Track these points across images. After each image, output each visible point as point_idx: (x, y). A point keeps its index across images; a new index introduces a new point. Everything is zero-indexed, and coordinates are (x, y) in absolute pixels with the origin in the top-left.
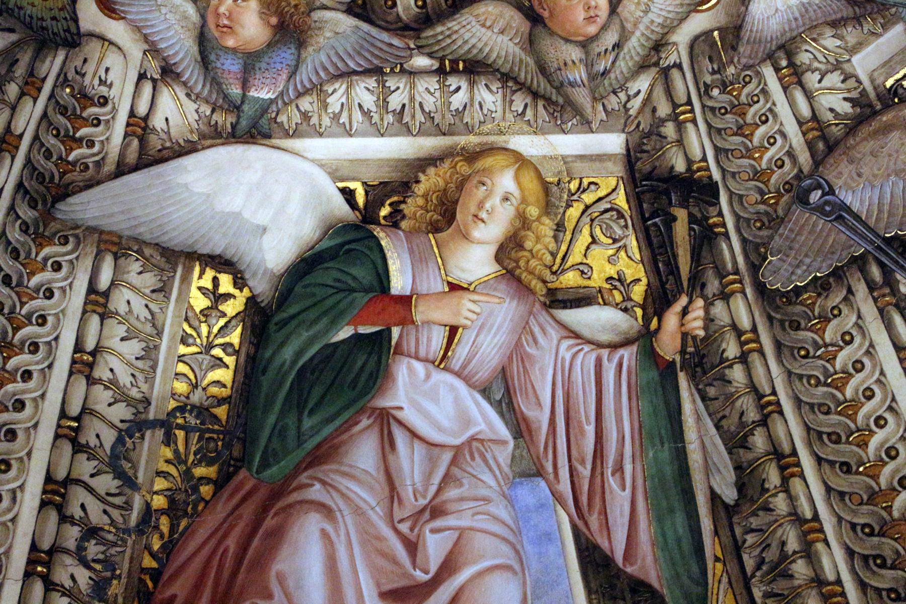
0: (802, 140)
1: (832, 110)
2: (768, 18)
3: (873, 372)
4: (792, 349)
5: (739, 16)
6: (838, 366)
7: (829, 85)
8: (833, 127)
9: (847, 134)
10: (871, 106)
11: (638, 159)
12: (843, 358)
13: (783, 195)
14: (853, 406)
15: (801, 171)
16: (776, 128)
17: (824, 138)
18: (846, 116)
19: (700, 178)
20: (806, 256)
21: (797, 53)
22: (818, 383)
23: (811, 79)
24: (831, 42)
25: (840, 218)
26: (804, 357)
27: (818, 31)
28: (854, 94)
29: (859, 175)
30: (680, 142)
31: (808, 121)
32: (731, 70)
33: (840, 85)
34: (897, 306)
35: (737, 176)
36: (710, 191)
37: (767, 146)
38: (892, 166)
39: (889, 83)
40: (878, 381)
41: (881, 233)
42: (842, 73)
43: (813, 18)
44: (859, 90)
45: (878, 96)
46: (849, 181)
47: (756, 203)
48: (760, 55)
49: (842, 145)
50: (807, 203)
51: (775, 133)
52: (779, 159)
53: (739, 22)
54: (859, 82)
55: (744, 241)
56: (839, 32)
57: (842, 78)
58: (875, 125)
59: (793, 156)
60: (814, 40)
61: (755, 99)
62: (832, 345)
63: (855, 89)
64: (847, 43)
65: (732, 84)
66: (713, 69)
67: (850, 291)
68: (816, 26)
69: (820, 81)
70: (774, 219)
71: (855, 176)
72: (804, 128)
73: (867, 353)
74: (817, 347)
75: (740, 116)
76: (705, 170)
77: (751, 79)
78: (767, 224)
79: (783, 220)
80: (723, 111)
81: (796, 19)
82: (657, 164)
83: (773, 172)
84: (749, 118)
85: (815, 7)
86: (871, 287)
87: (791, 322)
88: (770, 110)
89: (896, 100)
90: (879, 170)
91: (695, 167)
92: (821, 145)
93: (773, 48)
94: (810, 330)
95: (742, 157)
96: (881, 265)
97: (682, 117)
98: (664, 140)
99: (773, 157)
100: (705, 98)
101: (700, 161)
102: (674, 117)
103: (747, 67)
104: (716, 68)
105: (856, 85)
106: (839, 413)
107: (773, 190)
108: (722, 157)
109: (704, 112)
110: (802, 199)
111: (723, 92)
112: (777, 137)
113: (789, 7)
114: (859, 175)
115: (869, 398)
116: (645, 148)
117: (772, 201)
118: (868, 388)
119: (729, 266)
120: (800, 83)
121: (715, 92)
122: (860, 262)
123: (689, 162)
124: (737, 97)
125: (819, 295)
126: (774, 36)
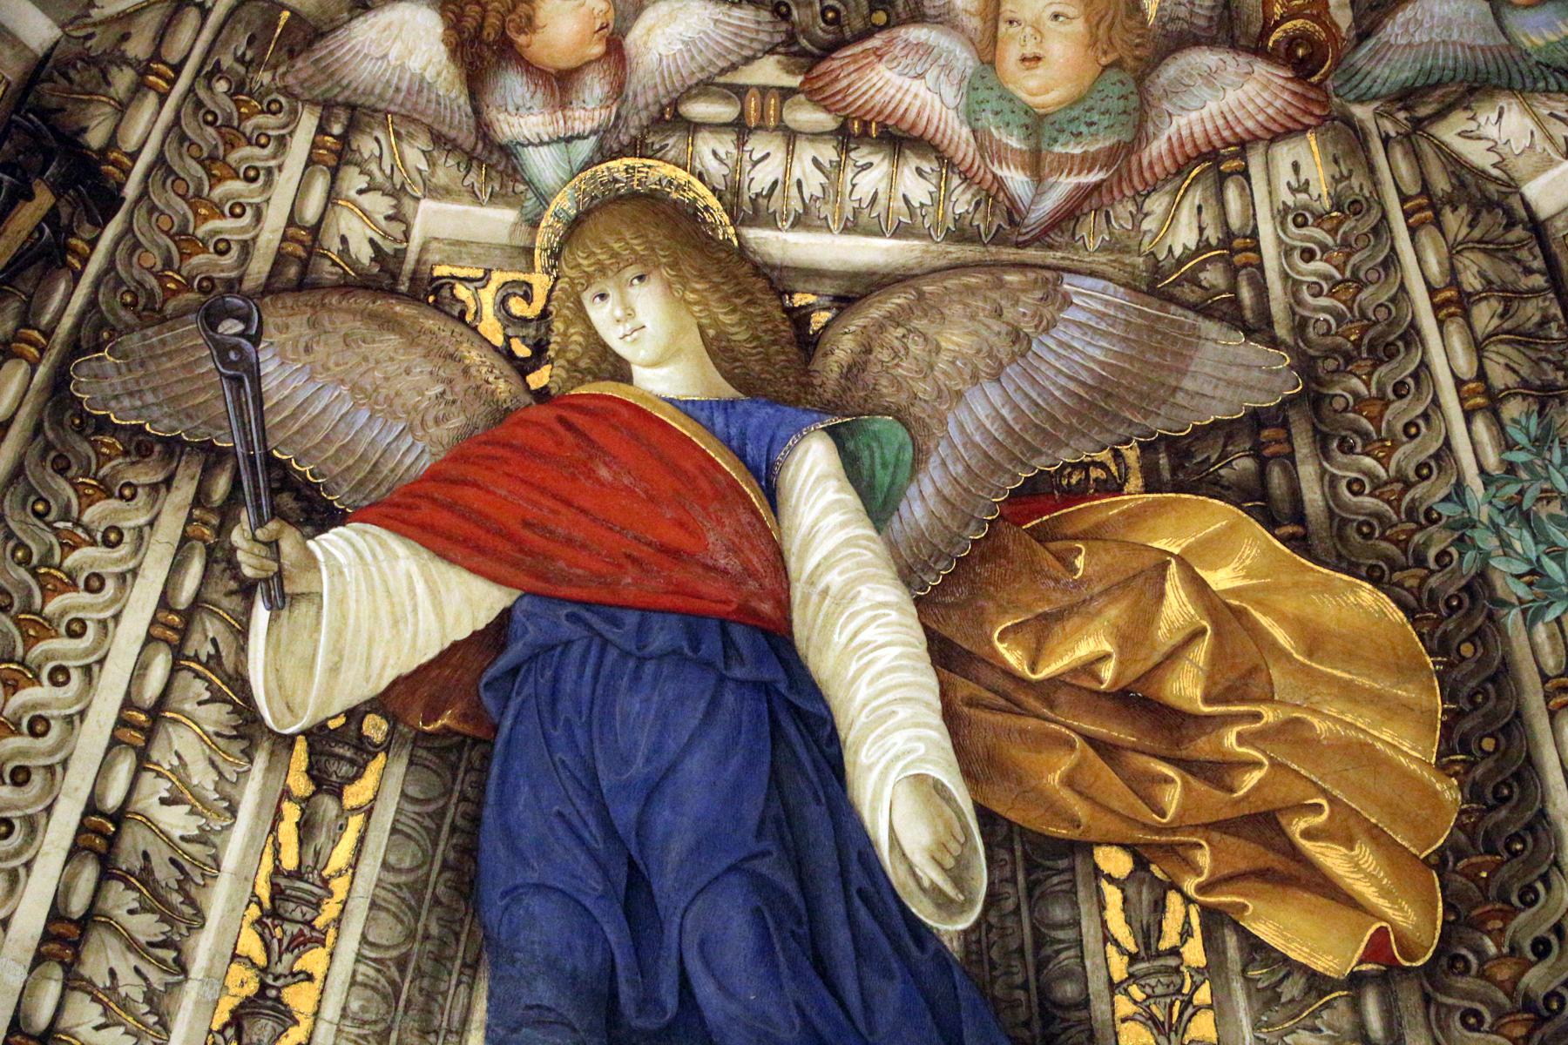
0: (276, 243)
1: (344, 240)
2: (366, 56)
3: (107, 606)
4: (32, 490)
5: (332, 21)
6: (68, 562)
7: (366, 206)
8: (328, 263)
9: (336, 287)
10: (395, 277)
11: (50, 79)
12: (84, 557)
13: (191, 290)
14: (46, 628)
15: (240, 280)
16: (257, 200)
17: (305, 265)
18: (354, 264)
19: (108, 175)
20: (154, 390)
21: (363, 132)
22: (25, 562)
23: (353, 180)
24: (414, 157)
25: (237, 381)
26: (40, 516)
27: (412, 128)
28: (388, 247)
29: (308, 350)
30: (122, 108)
31: (304, 228)
32: (265, 77)
33: (380, 218)
34: (210, 550)
35: (156, 215)
36: (108, 202)
37: (227, 210)
38: (355, 376)
39: (438, 272)
40: (103, 624)
41: (271, 444)
42: (395, 207)
43: (420, 108)
44: (398, 246)
45: (414, 278)
46: (289, 347)
47: (150, 270)
48: (317, 92)
49: (318, 295)
50: (214, 328)
51: (251, 204)
52: (227, 241)
53: (326, 28)
54: (407, 235)
55: (92, 303)
56: (435, 153)
57: (391, 212)
58: (380, 305)
59: (248, 253)
60: (397, 135)
61: (263, 140)
62: (87, 530)
63: (395, 240)
64: (433, 174)
65: (250, 94)
66: (244, 54)
67: (168, 482)
68: (414, 121)
69: (361, 192)
70: (153, 310)
71: (301, 346)
72: (291, 231)
73: (122, 577)
74: (65, 515)
75: (225, 143)
76: (123, 171)
77: (280, 110)
78: (140, 307)
79: (164, 320)
80: (210, 118)
81: (398, 90)
82: (69, 107)
83: (205, 250)
84: (233, 157)
85: (433, 97)
86: (200, 500)
87: (60, 456)
88: (269, 171)
89: (431, 299)
90: (337, 365)
91: (114, 155)
92: (292, 271)
93: (340, 99)
94: (75, 486)
95: (183, 197)
96: (236, 483)
97: (152, 78)
98: (104, 86)
99: (220, 232)
100: (201, 82)
101: (126, 154)
102: (143, 69)
103: (286, 91)
104: (248, 57)
105: (400, 236)
106: (17, 622)
107: (184, 273)
108: (158, 175)
109: (184, 98)
110: (211, 318)
111: (232, 94)
112: (249, 211)
113: (402, 66)
114: (308, 350)
115: (72, 634)
116: (72, 73)
117: (171, 286)
118: (82, 622)
119: (46, 318)
120: (335, 173)
121: (221, 86)
122: (212, 457)
123: (112, 141)
124: (243, 118)
125: (126, 453)
126: (354, 85)
